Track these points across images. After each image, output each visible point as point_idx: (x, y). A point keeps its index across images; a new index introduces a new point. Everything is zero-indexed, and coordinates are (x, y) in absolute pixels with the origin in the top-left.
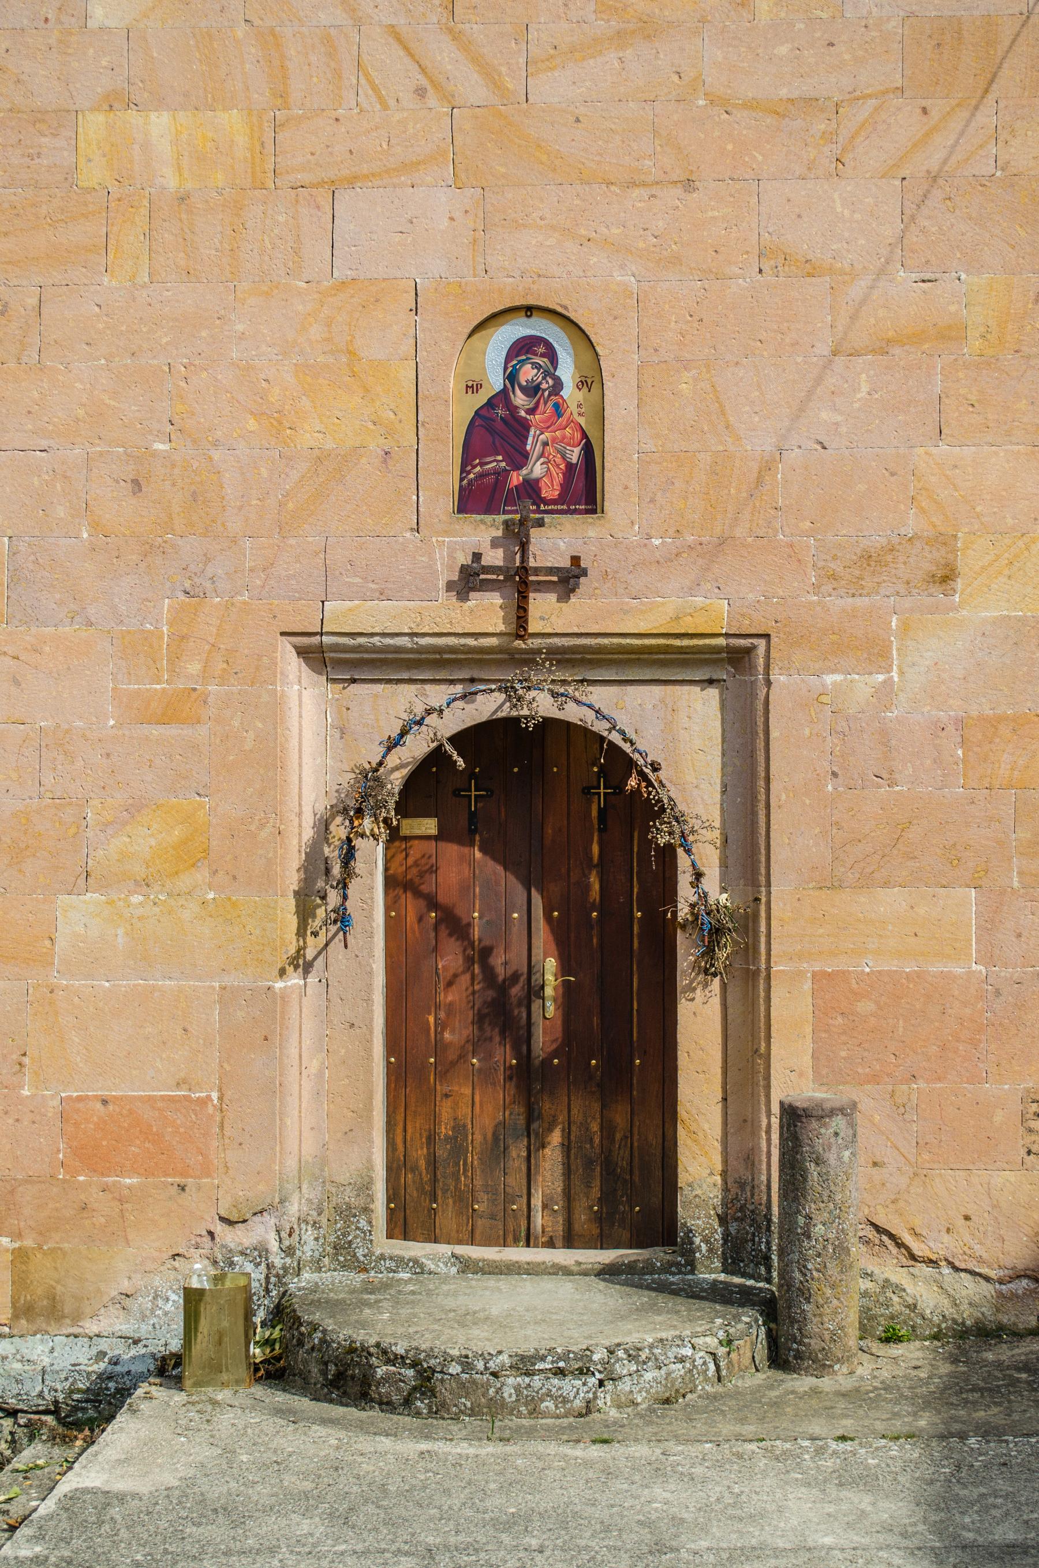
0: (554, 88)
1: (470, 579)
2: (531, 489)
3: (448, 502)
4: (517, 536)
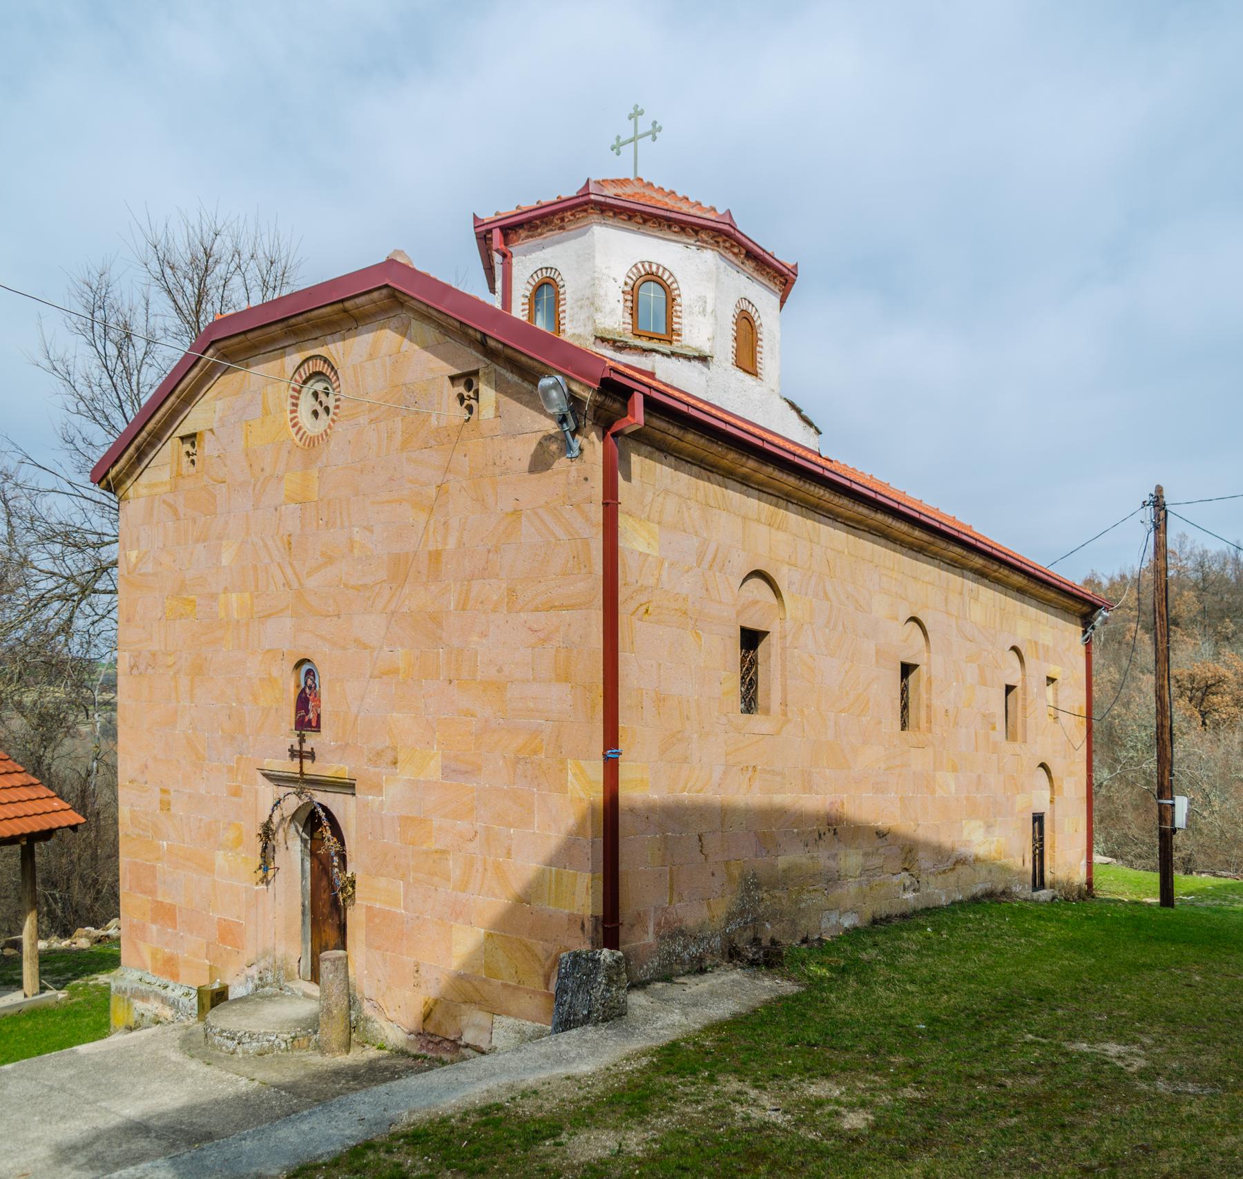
0: (311, 583)
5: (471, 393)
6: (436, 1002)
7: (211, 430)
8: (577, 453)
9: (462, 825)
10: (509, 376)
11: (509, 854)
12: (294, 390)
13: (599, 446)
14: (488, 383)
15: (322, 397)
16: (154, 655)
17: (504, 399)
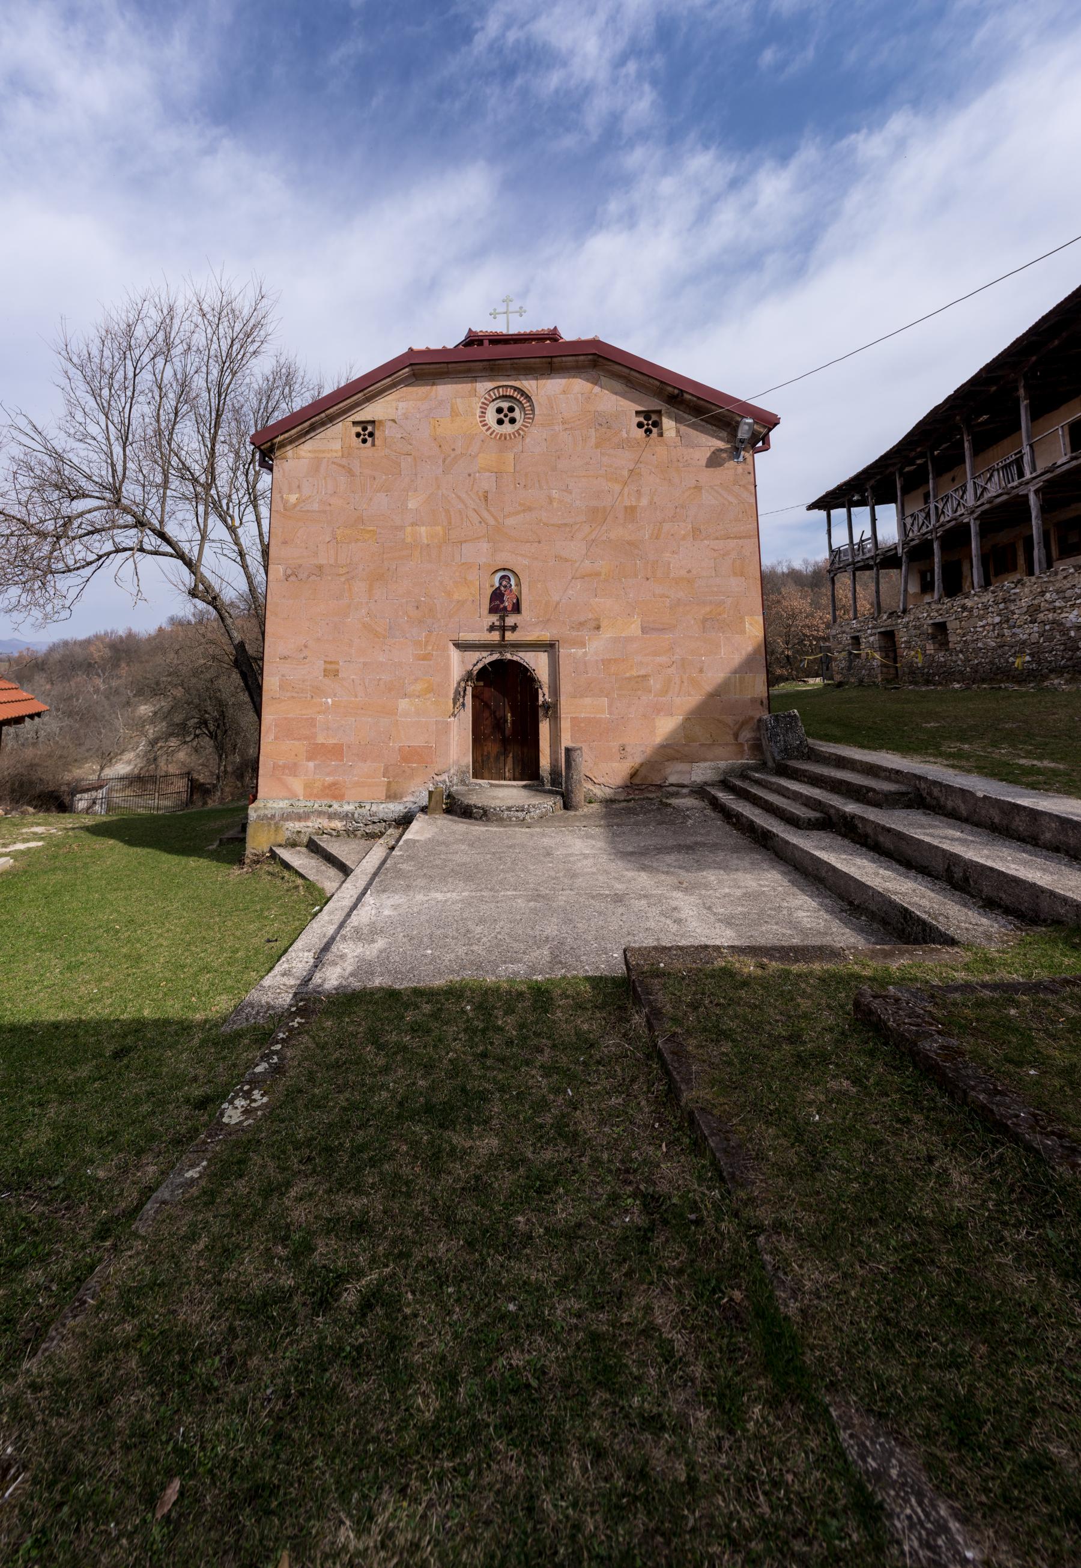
0: (510, 521)
1: (492, 628)
2: (505, 608)
3: (487, 611)
4: (502, 619)
7: (394, 421)
9: (663, 659)
11: (701, 671)
14: (670, 417)
16: (320, 567)
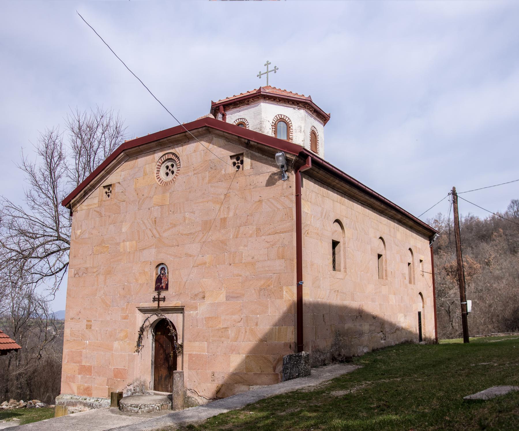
0: (165, 235)
5: (239, 162)
6: (222, 385)
7: (119, 183)
8: (286, 178)
9: (236, 317)
10: (257, 154)
11: (257, 324)
12: (158, 165)
13: (294, 175)
14: (248, 157)
15: (170, 167)
16: (87, 269)
17: (254, 162)
